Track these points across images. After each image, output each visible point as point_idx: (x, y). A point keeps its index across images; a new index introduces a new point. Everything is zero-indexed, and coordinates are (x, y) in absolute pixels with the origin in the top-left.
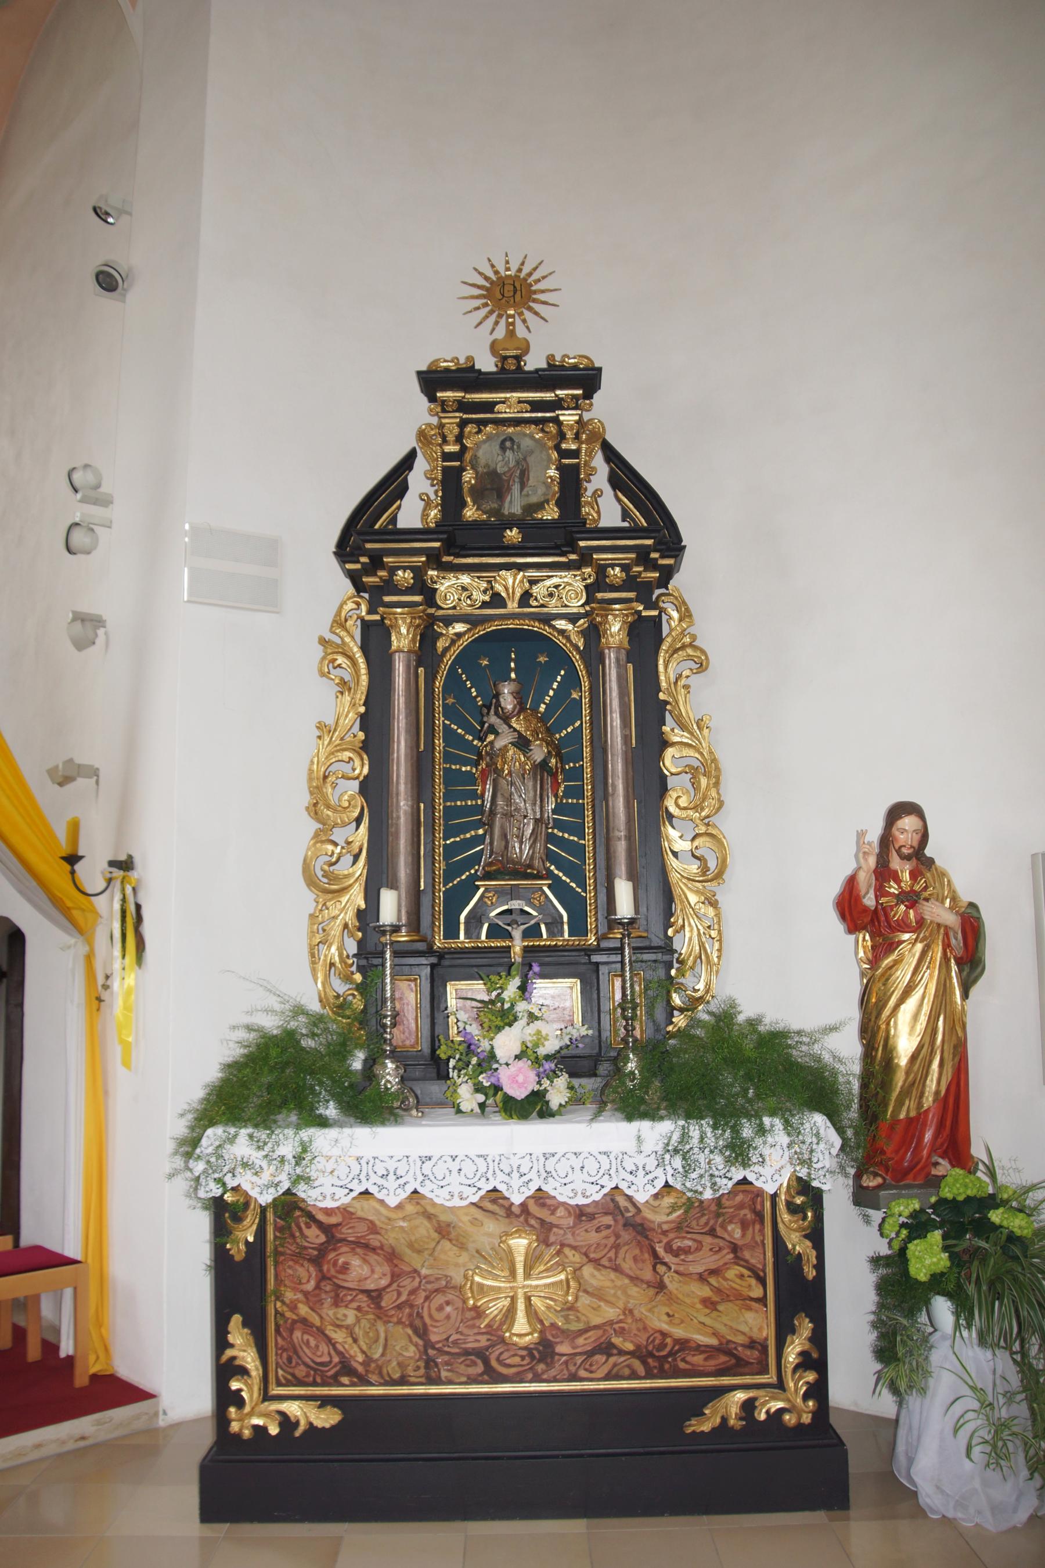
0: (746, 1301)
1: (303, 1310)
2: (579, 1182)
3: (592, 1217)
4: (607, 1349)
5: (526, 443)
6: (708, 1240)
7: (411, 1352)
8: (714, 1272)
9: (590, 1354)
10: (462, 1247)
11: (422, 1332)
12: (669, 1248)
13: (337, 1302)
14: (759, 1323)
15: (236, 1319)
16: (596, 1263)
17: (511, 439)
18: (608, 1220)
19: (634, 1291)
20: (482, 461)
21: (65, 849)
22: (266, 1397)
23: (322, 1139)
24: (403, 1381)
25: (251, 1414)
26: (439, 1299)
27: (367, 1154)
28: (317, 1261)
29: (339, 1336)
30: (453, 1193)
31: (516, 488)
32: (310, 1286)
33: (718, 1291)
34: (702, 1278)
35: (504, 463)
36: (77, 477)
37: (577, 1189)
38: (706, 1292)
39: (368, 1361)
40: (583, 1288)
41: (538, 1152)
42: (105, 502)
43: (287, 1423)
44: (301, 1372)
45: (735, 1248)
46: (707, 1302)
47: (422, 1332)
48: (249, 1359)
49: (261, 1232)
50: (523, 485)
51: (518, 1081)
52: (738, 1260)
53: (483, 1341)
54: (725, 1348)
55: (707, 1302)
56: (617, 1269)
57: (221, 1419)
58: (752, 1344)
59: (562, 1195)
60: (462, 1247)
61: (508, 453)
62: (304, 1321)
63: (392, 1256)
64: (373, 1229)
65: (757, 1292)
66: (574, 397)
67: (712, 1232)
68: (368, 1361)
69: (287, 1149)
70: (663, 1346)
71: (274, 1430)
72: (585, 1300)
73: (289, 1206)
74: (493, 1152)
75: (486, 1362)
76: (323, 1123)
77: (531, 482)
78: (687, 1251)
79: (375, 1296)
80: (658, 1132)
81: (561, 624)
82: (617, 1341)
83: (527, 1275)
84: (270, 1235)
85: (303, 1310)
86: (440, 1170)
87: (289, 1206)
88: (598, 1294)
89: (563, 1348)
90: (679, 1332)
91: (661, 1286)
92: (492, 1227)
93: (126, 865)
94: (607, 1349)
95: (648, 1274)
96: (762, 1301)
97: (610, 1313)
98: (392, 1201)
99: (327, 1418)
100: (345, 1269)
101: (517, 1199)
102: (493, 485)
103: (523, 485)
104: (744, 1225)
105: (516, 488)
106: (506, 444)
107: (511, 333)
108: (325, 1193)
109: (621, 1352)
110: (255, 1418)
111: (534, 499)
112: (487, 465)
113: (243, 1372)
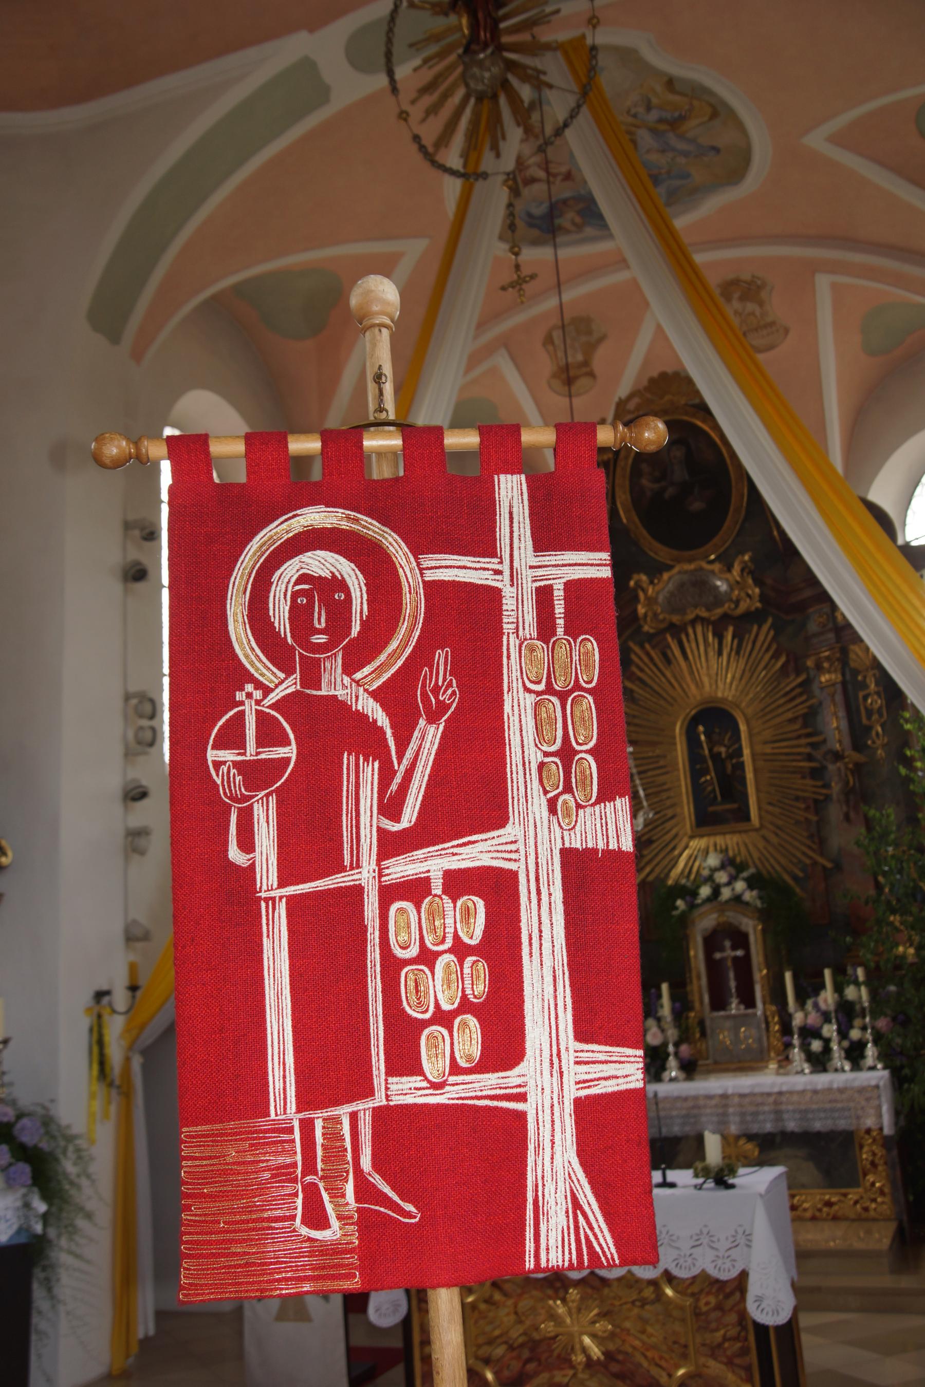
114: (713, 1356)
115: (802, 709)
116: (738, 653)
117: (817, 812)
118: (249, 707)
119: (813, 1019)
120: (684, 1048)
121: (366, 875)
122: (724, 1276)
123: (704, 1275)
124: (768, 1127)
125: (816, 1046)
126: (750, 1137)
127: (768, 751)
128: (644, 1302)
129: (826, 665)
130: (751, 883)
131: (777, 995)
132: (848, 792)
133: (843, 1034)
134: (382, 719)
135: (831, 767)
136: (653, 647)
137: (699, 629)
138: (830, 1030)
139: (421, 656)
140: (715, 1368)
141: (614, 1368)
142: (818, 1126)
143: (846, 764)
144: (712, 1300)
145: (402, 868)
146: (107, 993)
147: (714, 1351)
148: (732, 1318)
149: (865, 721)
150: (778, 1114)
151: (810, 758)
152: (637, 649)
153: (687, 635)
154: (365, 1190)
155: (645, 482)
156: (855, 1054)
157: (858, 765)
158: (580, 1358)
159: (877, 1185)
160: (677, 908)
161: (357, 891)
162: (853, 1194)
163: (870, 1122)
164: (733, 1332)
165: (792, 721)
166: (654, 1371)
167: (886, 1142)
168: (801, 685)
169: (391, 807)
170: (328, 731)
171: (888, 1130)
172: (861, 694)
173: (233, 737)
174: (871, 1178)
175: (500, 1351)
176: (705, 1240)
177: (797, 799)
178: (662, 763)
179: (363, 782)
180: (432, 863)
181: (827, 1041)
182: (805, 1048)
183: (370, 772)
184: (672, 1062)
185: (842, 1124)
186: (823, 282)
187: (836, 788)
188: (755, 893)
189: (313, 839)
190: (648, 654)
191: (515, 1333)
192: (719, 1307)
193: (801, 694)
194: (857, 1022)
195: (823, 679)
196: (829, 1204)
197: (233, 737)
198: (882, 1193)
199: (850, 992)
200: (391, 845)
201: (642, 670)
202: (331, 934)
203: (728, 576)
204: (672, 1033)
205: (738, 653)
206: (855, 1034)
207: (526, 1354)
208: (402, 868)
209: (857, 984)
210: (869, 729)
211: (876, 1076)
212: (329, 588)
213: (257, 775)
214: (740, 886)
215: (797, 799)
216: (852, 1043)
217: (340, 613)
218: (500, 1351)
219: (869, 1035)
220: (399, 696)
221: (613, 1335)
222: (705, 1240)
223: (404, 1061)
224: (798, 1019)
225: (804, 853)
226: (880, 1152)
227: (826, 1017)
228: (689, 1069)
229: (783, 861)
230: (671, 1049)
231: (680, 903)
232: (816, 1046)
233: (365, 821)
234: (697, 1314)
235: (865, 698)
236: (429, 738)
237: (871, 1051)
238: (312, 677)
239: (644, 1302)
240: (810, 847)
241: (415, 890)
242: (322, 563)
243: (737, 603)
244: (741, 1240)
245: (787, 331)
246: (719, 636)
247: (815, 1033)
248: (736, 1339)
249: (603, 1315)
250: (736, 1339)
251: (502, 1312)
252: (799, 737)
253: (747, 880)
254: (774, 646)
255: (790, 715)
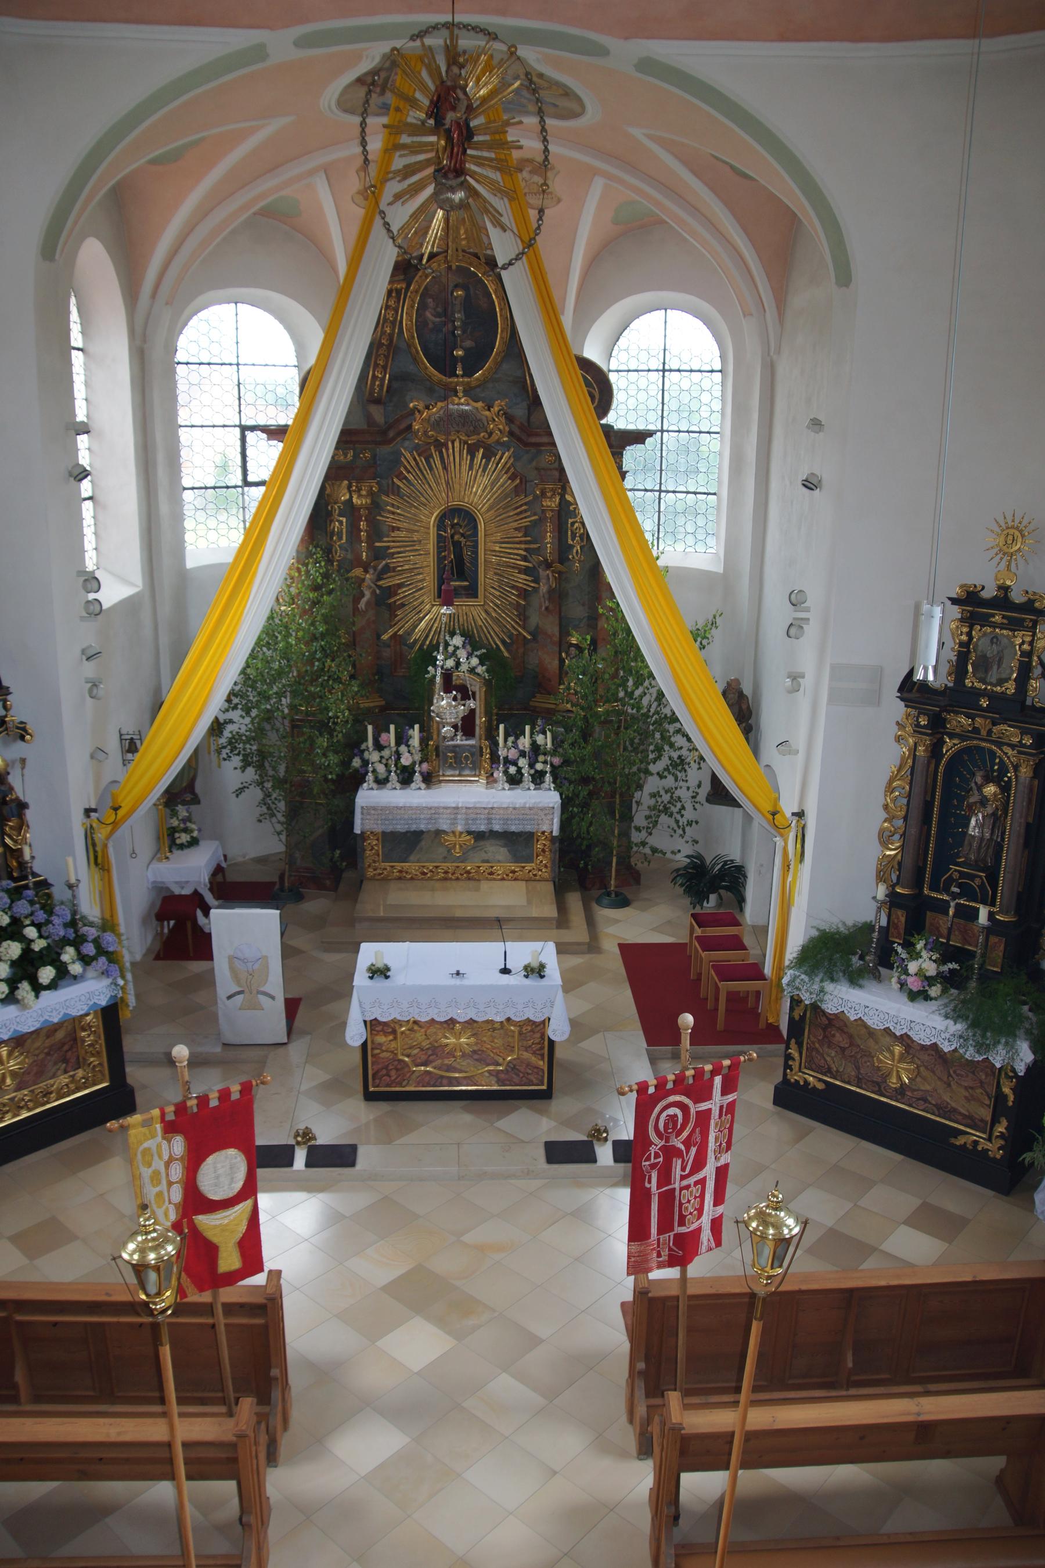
0: (982, 1104)
1: (817, 1045)
2: (922, 1035)
3: (927, 1050)
4: (925, 1101)
5: (1005, 641)
6: (971, 1075)
7: (853, 1073)
8: (972, 1088)
9: (919, 1099)
10: (877, 1043)
11: (858, 1068)
12: (955, 1072)
13: (829, 1047)
14: (986, 1114)
15: (793, 1041)
16: (926, 1068)
17: (996, 637)
18: (933, 1053)
19: (939, 1083)
20: (980, 648)
21: (769, 807)
22: (800, 1070)
23: (829, 987)
24: (849, 1083)
25: (795, 1074)
26: (865, 1059)
27: (845, 998)
28: (824, 1029)
29: (828, 1059)
30: (874, 1022)
31: (995, 667)
32: (820, 1038)
33: (972, 1096)
34: (966, 1088)
35: (991, 651)
36: (793, 596)
37: (922, 1037)
38: (967, 1094)
39: (837, 1071)
40: (919, 1073)
41: (909, 1018)
42: (807, 610)
43: (806, 1081)
44: (814, 1066)
45: (981, 1082)
46: (966, 1097)
47: (858, 1068)
48: (796, 1055)
49: (805, 1011)
50: (999, 667)
51: (914, 984)
52: (982, 1087)
53: (879, 1080)
54: (970, 1117)
55: (966, 1097)
56: (933, 1072)
57: (785, 1074)
58: (982, 1120)
59: (915, 1038)
60: (877, 1043)
61: (994, 646)
62: (817, 1049)
63: (851, 1037)
64: (846, 1025)
65: (987, 1102)
66: (1031, 620)
67: (973, 1073)
68: (837, 1071)
69: (816, 987)
70: (946, 1107)
71: (802, 1083)
72: (919, 1079)
73: (815, 1007)
74: (892, 1013)
75: (880, 1087)
76: (832, 980)
77: (1004, 666)
78: (962, 1076)
79: (843, 1049)
80: (959, 1027)
81: (1006, 749)
82: (929, 1098)
83: (899, 1062)
84: (808, 1015)
85: (817, 1045)
86: (871, 1013)
87: (816, 1008)
88: (924, 1079)
89: (909, 1093)
90: (954, 1105)
91: (949, 1085)
92: (888, 1039)
93: (800, 815)
94: (925, 1101)
95: (945, 1079)
96: (989, 1106)
97: (928, 1088)
98: (852, 1019)
99: (820, 1086)
100: (834, 1036)
101: (898, 1034)
102: (984, 665)
103: (999, 667)
104: (987, 1075)
105: (995, 667)
106: (994, 640)
107: (1008, 567)
108: (830, 1007)
109: (930, 1103)
110: (795, 1077)
111: (1004, 676)
112: (982, 651)
113: (793, 1059)
114: (526, 1051)
115: (525, 522)
116: (484, 471)
117: (525, 600)
118: (653, 1149)
119: (513, 754)
120: (425, 766)
121: (677, 1186)
122: (538, 1020)
123: (528, 1020)
124: (483, 828)
125: (512, 770)
126: (469, 833)
127: (497, 549)
128: (494, 1029)
129: (549, 495)
130: (482, 661)
131: (491, 735)
132: (551, 591)
133: (531, 766)
134: (683, 1148)
135: (543, 573)
136: (419, 455)
137: (457, 444)
138: (523, 762)
139: (693, 1131)
140: (526, 1055)
141: (476, 1057)
142: (513, 828)
143: (553, 572)
144: (529, 1028)
145: (685, 1183)
146: (95, 810)
147: (526, 1049)
148: (538, 1035)
149: (570, 542)
150: (489, 820)
151: (525, 559)
152: (408, 455)
153: (447, 449)
154: (670, 1249)
155: (428, 314)
156: (538, 778)
157: (560, 573)
158: (459, 1054)
159: (543, 863)
160: (428, 672)
161: (674, 1189)
162: (529, 867)
163: (545, 828)
164: (537, 1041)
165: (516, 529)
166: (497, 1058)
167: (553, 839)
168: (526, 504)
169: (683, 1169)
170: (670, 1153)
171: (556, 833)
172: (570, 521)
173: (648, 1159)
174: (540, 858)
175: (416, 1051)
176: (530, 1005)
177: (513, 587)
178: (417, 547)
179: (677, 1164)
180: (692, 1180)
181: (519, 770)
182: (506, 772)
183: (679, 1162)
184: (417, 777)
185: (529, 828)
186: (598, 185)
187: (543, 589)
188: (484, 668)
189: (665, 1177)
190: (415, 459)
191: (425, 1044)
192: (532, 1031)
193: (525, 511)
194: (541, 758)
195: (544, 504)
196: (514, 872)
197: (648, 1159)
198: (546, 866)
199: (540, 739)
200: (683, 1178)
201: (409, 472)
202: (668, 1200)
203: (487, 413)
204: (417, 757)
205: (484, 471)
206: (539, 766)
207: (430, 1052)
208: (685, 1183)
209: (544, 733)
210: (571, 547)
211: (550, 798)
212: (673, 1118)
213: (653, 1166)
214: (475, 661)
215: (513, 587)
216: (537, 771)
217: (675, 1123)
218: (416, 1051)
219: (548, 768)
220: (687, 1143)
221: (476, 1044)
222: (530, 1005)
223: (682, 1223)
224: (502, 752)
225: (514, 627)
226: (548, 843)
227: (523, 754)
228: (429, 779)
229: (497, 629)
230: (417, 768)
231: (430, 668)
232: (512, 770)
233: (677, 1172)
234: (520, 1033)
235: (573, 524)
236: (693, 1150)
237: (548, 778)
238: (667, 1141)
239: (494, 1029)
240: (517, 622)
241: (687, 1187)
242: (672, 1111)
243: (490, 434)
244: (549, 1004)
245: (559, 201)
246: (472, 453)
247: (515, 763)
248: (538, 1044)
249: (473, 1035)
250: (538, 1044)
251: (418, 1035)
252: (520, 543)
253: (479, 657)
254: (512, 470)
255: (515, 525)
